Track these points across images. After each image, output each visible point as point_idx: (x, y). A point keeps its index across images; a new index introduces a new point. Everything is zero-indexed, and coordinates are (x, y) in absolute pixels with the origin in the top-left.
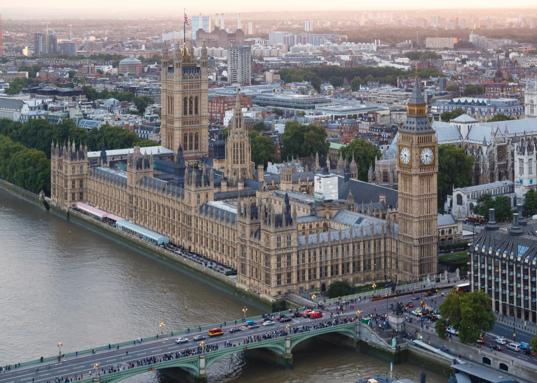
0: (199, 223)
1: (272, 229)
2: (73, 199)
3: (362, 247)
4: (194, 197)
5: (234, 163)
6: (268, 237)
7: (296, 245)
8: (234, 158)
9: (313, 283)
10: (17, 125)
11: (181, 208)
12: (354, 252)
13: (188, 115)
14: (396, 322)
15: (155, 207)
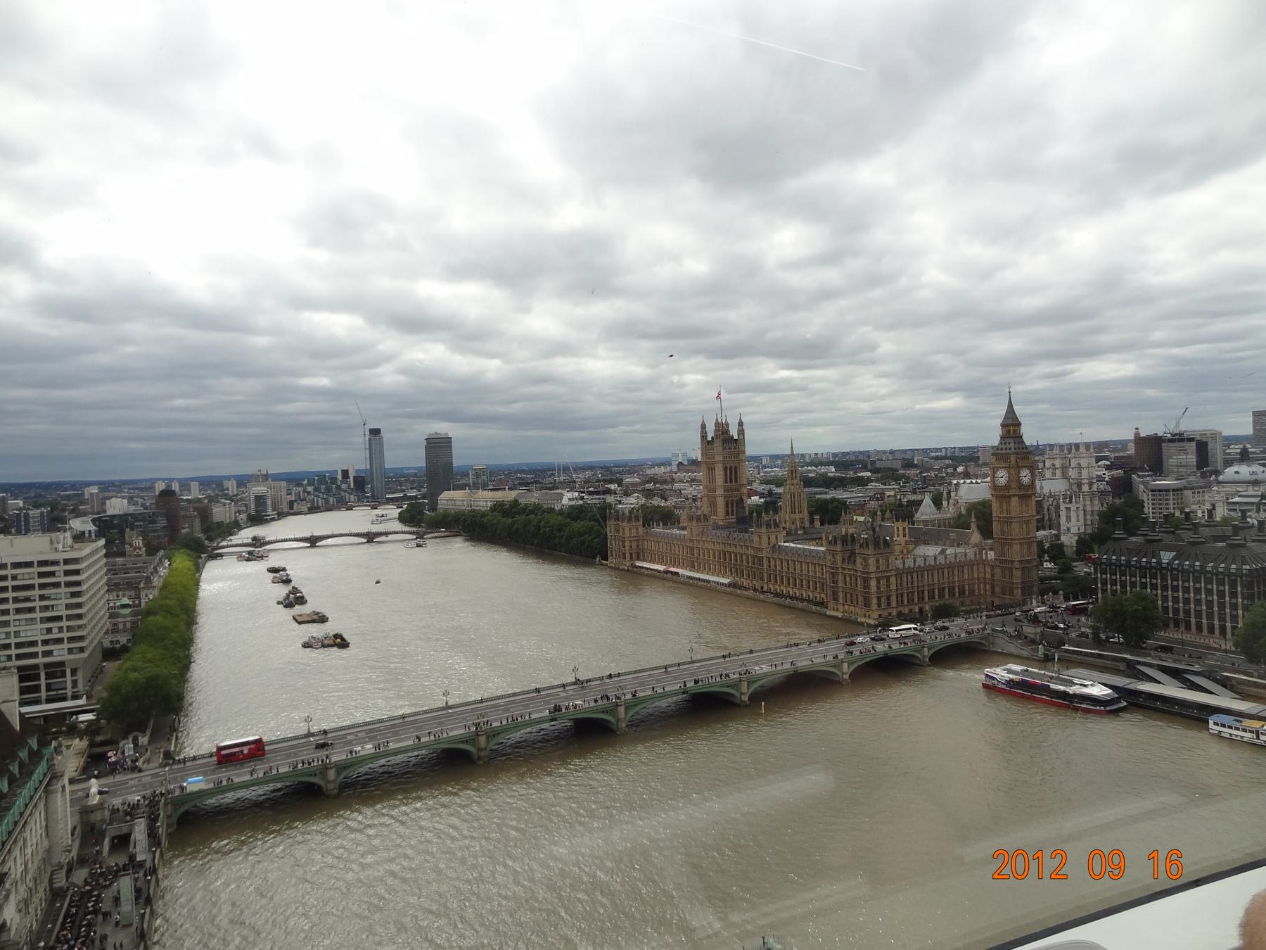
0: (772, 563)
1: (871, 551)
2: (631, 558)
3: (956, 572)
4: (764, 539)
5: (792, 513)
6: (865, 560)
7: (894, 568)
8: (792, 508)
9: (911, 607)
10: (561, 512)
11: (751, 551)
12: (948, 577)
13: (729, 484)
14: (1033, 632)
15: (720, 554)
